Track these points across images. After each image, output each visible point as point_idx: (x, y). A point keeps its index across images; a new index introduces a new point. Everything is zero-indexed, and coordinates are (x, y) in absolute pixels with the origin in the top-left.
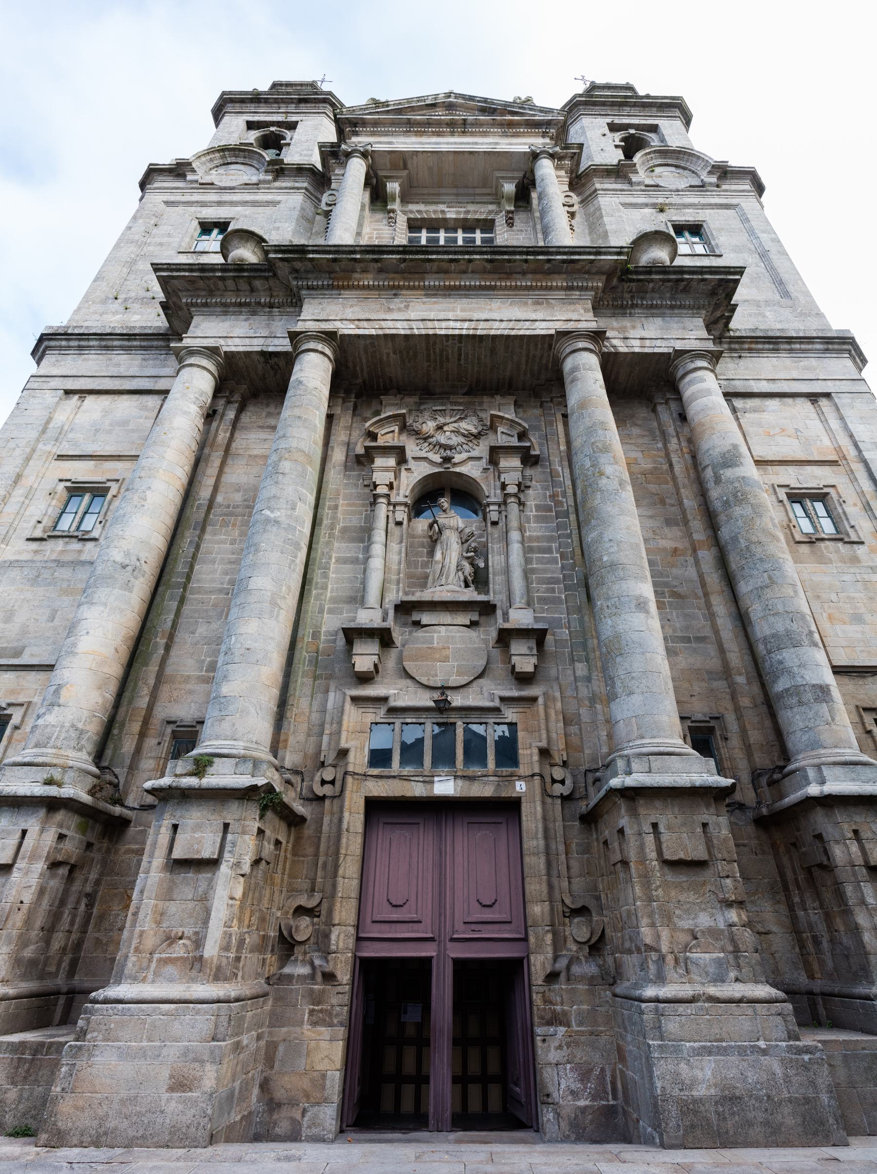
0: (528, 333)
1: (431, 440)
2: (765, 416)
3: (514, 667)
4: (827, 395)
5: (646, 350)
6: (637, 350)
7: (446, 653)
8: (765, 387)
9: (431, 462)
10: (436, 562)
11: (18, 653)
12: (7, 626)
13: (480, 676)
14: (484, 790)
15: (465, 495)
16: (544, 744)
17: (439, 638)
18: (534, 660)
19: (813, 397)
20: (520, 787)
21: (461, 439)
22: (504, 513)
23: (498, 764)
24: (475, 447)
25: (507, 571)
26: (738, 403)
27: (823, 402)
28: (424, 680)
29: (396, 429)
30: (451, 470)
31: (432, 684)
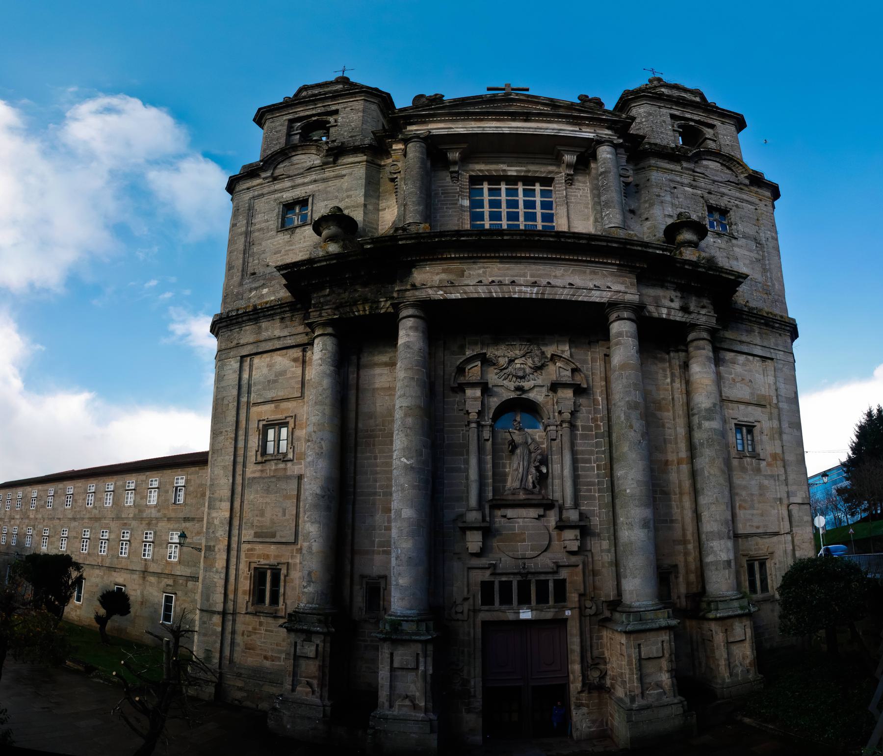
1: (505, 371)
3: (565, 547)
9: (507, 389)
13: (545, 551)
14: (549, 615)
15: (531, 409)
16: (582, 591)
17: (519, 527)
18: (578, 543)
20: (568, 613)
21: (528, 370)
22: (560, 433)
24: (540, 377)
25: (562, 477)
29: (479, 363)
30: (523, 396)
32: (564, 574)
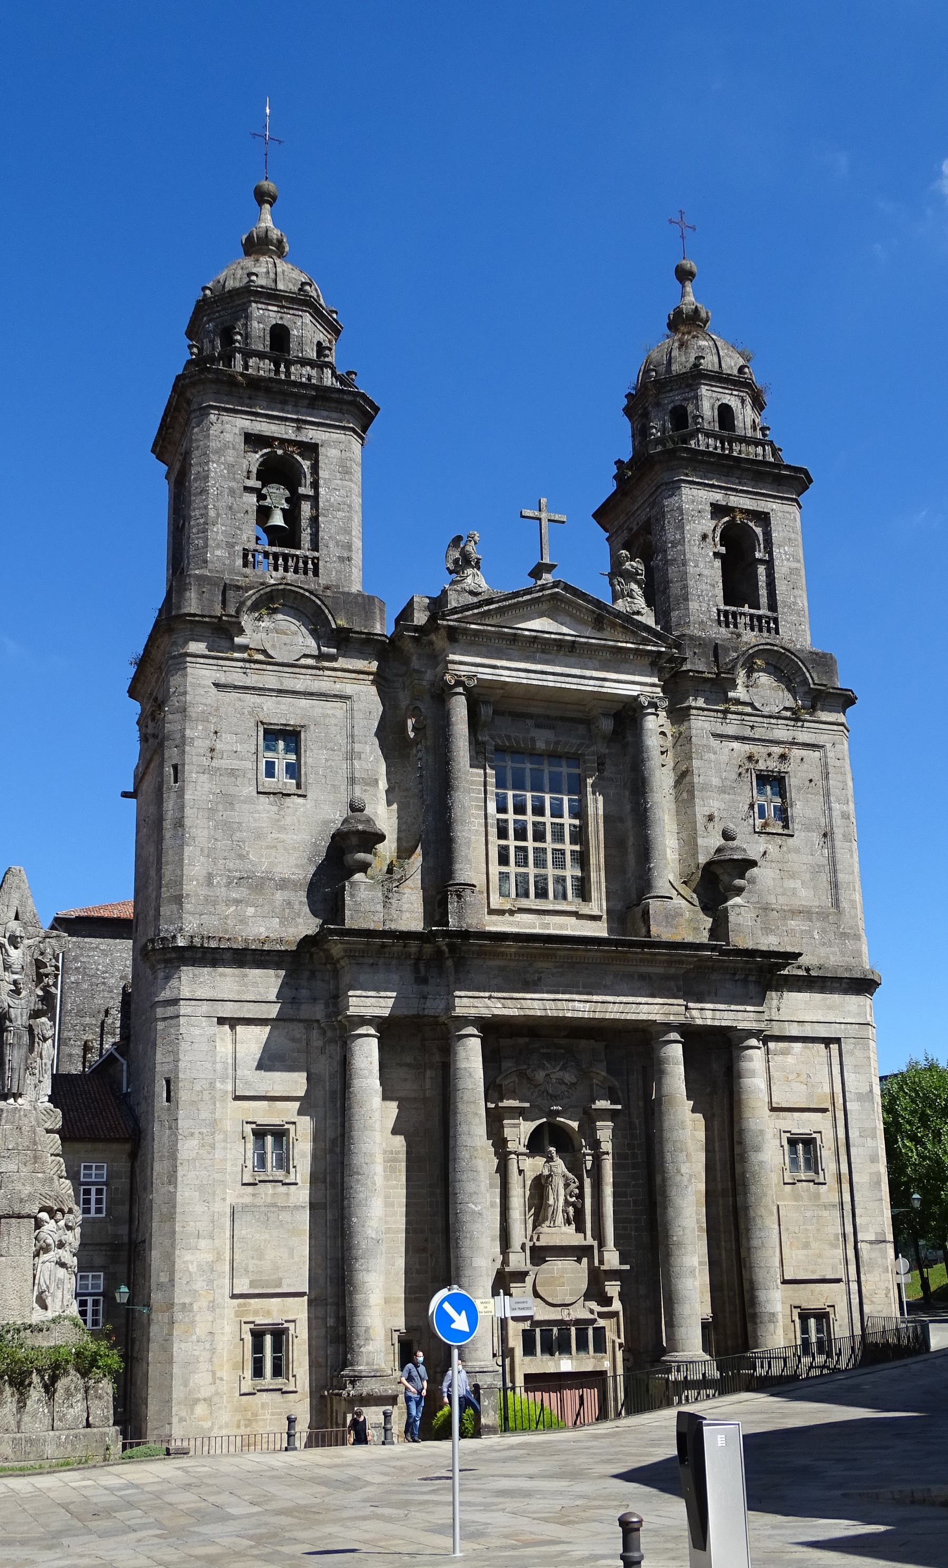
0: (633, 1017)
2: (790, 1059)
4: (838, 1040)
5: (717, 1023)
6: (709, 1022)
7: (561, 1280)
8: (794, 1031)
10: (550, 1206)
11: (279, 1285)
12: (262, 1262)
19: (827, 1042)
23: (595, 1351)
26: (772, 1045)
27: (834, 1047)
28: (550, 1300)
31: (555, 1303)
32: (601, 1323)
